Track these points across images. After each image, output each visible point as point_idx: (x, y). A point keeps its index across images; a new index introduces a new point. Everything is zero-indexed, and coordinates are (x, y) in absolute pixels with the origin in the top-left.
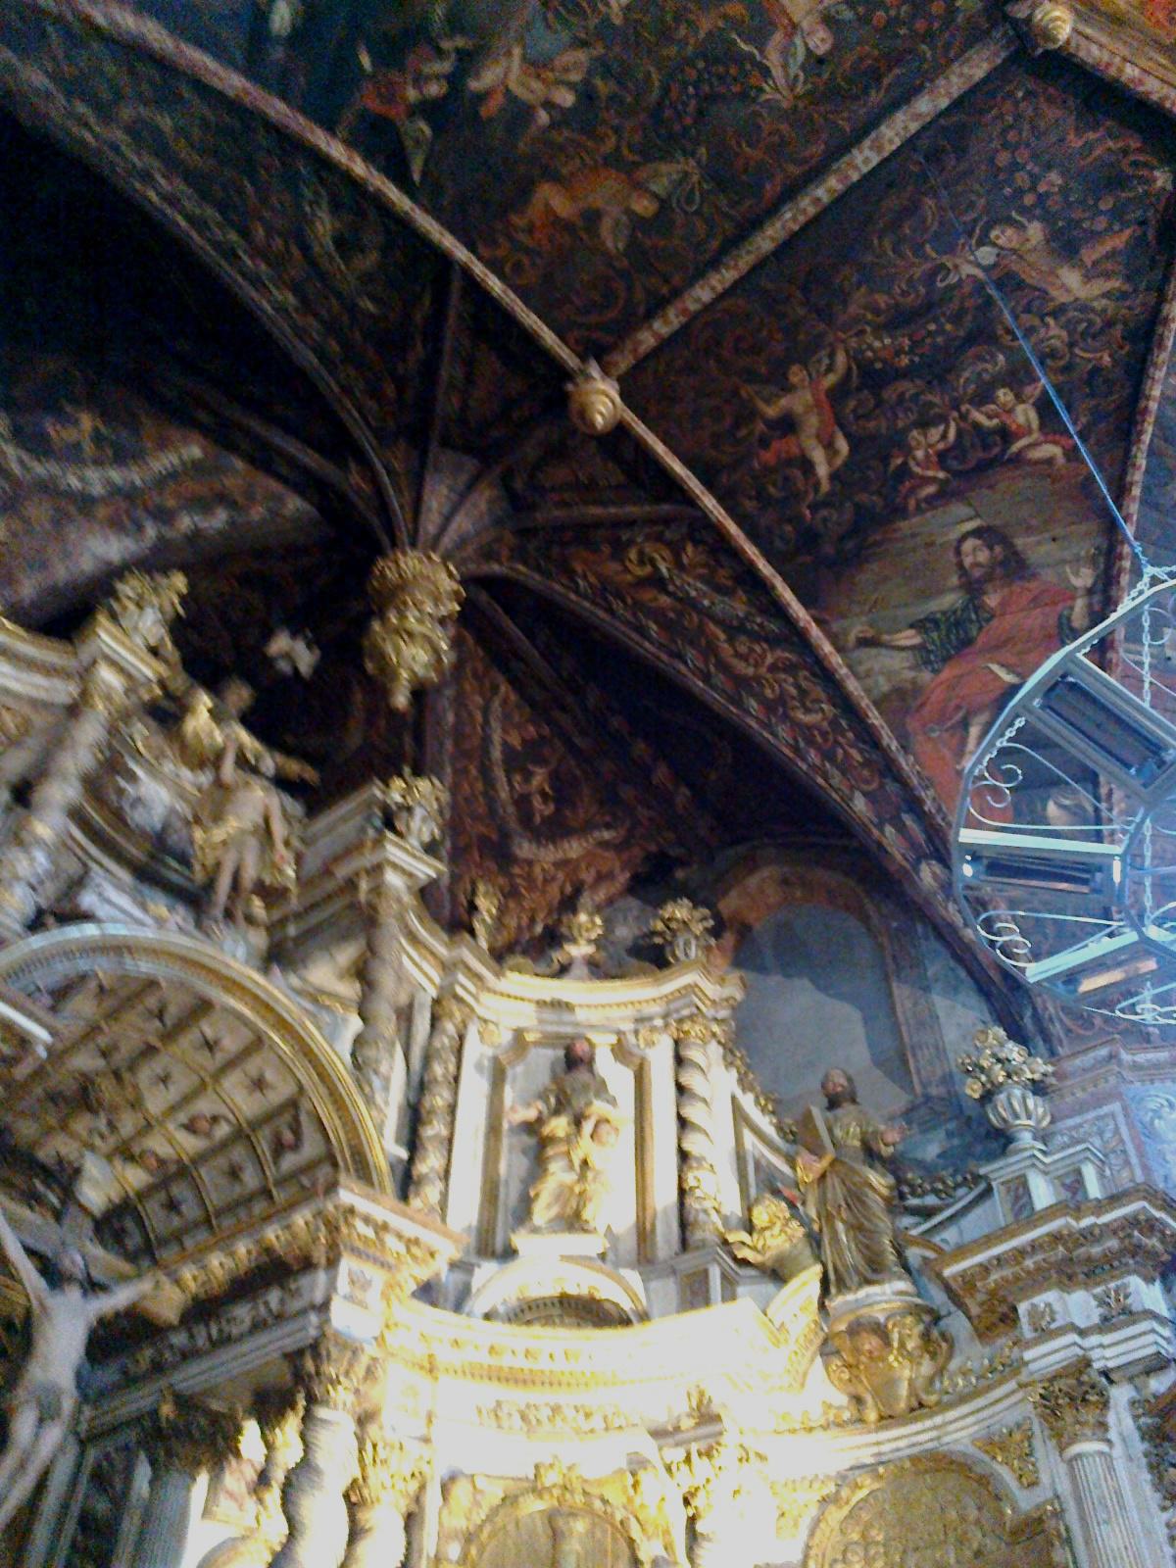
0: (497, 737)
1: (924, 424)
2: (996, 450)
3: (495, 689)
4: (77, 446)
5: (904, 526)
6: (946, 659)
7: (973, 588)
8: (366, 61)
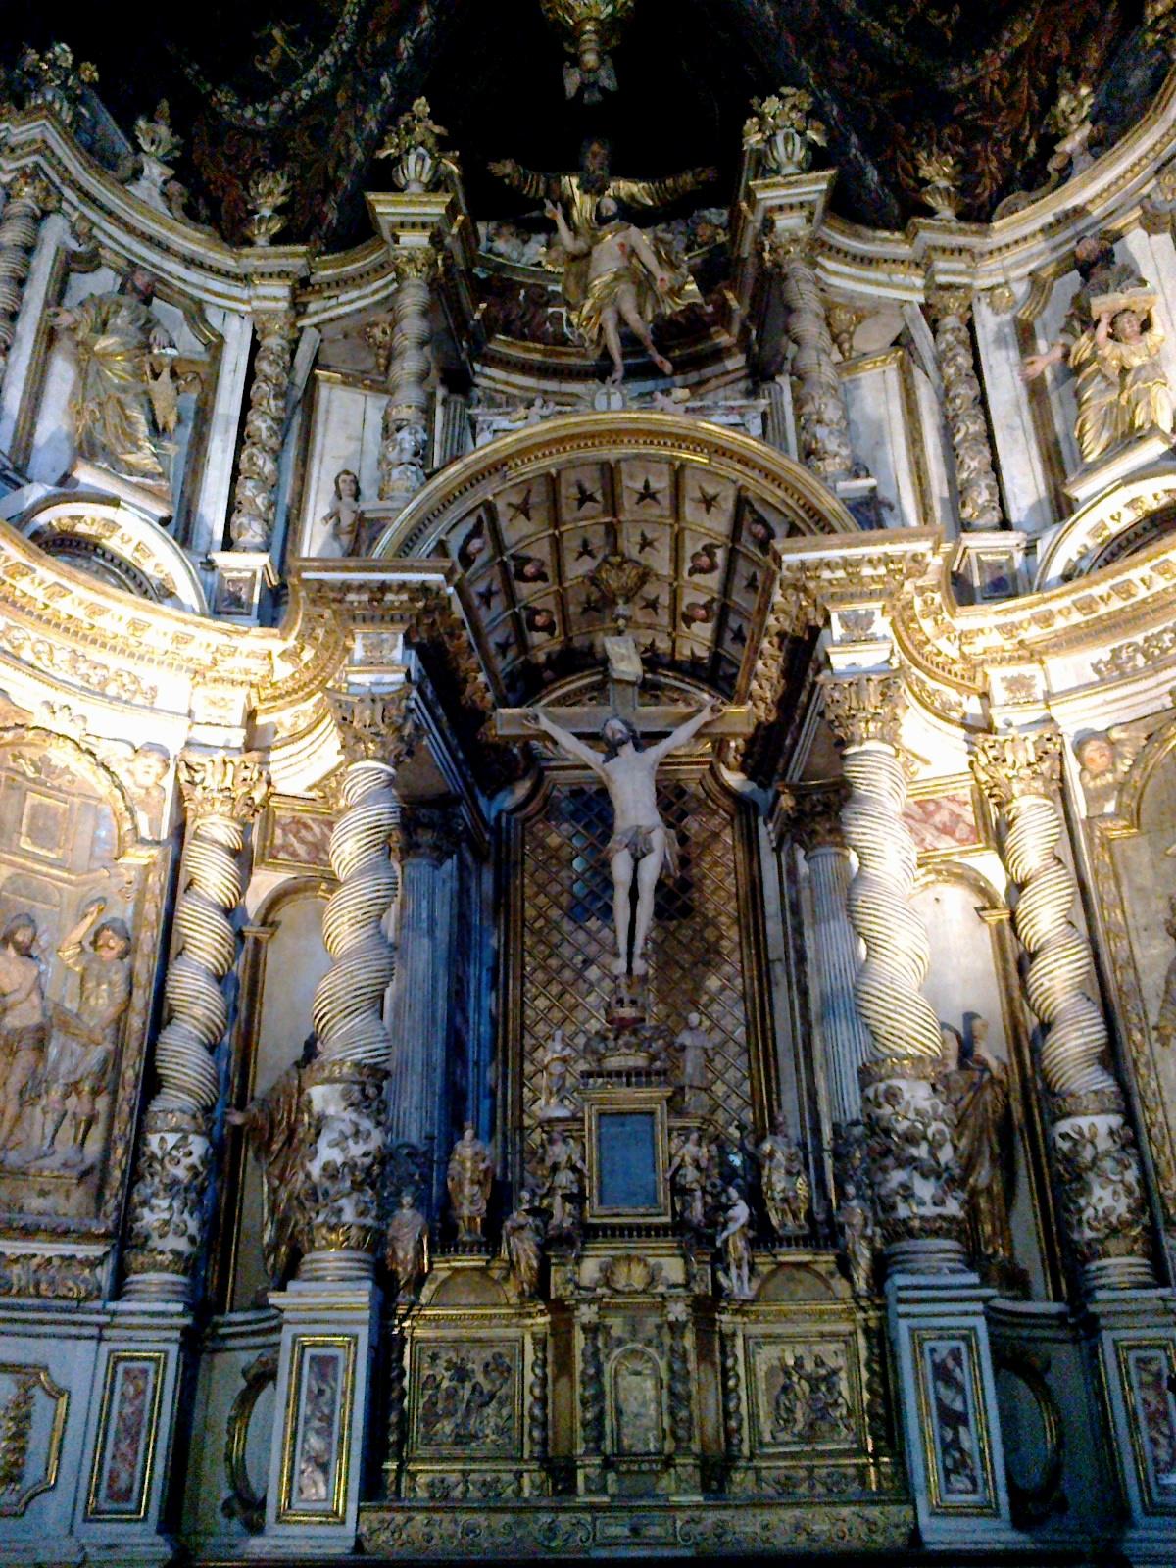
4: (285, 60)
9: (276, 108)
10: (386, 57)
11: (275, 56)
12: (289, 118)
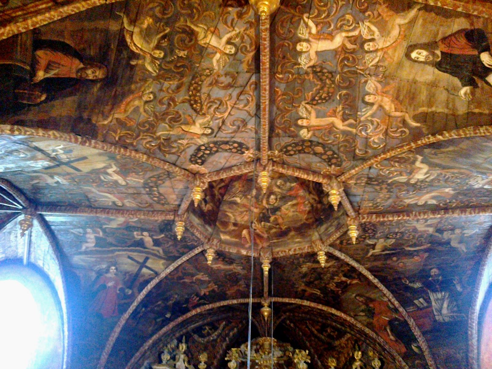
0: (313, 330)
1: (328, 284)
3: (306, 323)
4: (208, 332)
6: (373, 317)
9: (206, 340)
10: (227, 335)
11: (206, 331)
12: (208, 342)
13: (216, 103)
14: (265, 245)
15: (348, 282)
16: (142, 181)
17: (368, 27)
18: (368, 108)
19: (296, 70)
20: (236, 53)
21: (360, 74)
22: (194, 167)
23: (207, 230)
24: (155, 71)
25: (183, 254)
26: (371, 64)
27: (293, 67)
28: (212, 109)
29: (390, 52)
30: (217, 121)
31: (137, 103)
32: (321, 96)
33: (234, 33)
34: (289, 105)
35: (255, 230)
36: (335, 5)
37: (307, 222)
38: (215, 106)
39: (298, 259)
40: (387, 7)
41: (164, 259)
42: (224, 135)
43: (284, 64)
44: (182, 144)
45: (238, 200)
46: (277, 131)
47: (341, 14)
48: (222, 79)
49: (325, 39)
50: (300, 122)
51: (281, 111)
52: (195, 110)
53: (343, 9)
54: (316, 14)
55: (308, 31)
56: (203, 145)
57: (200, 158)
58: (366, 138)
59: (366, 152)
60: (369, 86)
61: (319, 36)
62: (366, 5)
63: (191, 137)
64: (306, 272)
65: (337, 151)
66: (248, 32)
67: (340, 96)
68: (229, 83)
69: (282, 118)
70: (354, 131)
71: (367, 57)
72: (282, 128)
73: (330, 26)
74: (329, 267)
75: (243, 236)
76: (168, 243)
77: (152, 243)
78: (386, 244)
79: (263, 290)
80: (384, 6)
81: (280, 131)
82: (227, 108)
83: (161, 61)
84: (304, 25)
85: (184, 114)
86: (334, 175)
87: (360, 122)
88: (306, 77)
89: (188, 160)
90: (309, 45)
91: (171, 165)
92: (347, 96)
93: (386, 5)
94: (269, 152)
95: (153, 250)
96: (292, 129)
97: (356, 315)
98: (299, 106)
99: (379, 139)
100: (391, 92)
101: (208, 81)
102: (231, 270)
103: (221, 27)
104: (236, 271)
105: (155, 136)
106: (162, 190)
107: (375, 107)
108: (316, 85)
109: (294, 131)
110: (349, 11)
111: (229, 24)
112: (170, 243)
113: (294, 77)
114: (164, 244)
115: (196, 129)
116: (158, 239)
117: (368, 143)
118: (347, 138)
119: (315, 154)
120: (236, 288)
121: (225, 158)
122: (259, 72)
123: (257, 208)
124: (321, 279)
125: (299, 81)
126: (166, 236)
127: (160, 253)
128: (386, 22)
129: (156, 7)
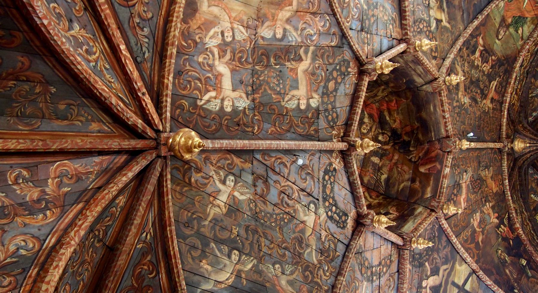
1: (484, 72)
2: (484, 52)
3: (532, 97)
5: (500, 56)
6: (524, 18)
7: (508, 27)
8: (511, 243)
13: (283, 197)
14: (438, 146)
15: (482, 48)
16: (365, 283)
17: (210, 38)
18: (288, 34)
19: (251, 112)
20: (234, 175)
21: (255, 44)
22: (350, 223)
23: (420, 213)
24: (252, 261)
25: (449, 241)
26: (245, 34)
27: (246, 114)
28: (289, 202)
29: (234, 15)
30: (302, 197)
31: (283, 282)
32: (277, 85)
33: (215, 176)
34: (285, 119)
35: (420, 157)
36: (190, 73)
37: (411, 97)
38: (286, 198)
39: (454, 108)
40: (192, 20)
41: (454, 264)
42: (317, 189)
43: (244, 124)
44: (326, 237)
45: (384, 177)
46: (312, 132)
47: (197, 66)
48: (259, 190)
49: (221, 82)
50: (303, 107)
51: (291, 127)
52: (290, 221)
53: (194, 65)
54: (198, 92)
55: (213, 100)
56: (327, 214)
57: (340, 217)
58: (320, 35)
59: (334, 34)
60: (266, 34)
61: (218, 88)
62: (190, 41)
63: (318, 225)
64: (469, 98)
65: (333, 66)
66: (214, 162)
67: (276, 65)
68: (263, 183)
69: (298, 126)
70: (312, 48)
71: (238, 37)
72: (309, 126)
73: (209, 77)
74: (463, 71)
75: (427, 172)
76: (436, 259)
77: (435, 277)
78: (436, 7)
79: (492, 149)
80: (191, 23)
81: (312, 129)
82: (288, 186)
83: (242, 254)
84: (208, 104)
85: (294, 232)
86: (359, 68)
87: (302, 42)
88: (258, 101)
89: (344, 231)
90: (227, 99)
91: (349, 250)
92: (277, 57)
93: (190, 21)
94: (334, 140)
95: (443, 276)
96: (310, 115)
97: (522, 39)
98: (286, 108)
99: (320, 21)
100: (273, 11)
101: (260, 205)
102: (468, 186)
103: (209, 189)
104: (469, 180)
105: (318, 266)
106: (376, 262)
107: (288, 27)
108: (265, 90)
109: (313, 114)
110: (195, 58)
111: (207, 181)
112: (436, 256)
113: (257, 114)
114: (436, 263)
115: (310, 219)
116: (431, 269)
117: (325, 32)
118: (319, 55)
119: (336, 90)
120: (489, 181)
121: (340, 190)
122: (253, 151)
123: (393, 156)
124: (478, 80)
125: (261, 108)
126: (427, 260)
127: (447, 269)
128: (205, 19)
129: (192, 255)
